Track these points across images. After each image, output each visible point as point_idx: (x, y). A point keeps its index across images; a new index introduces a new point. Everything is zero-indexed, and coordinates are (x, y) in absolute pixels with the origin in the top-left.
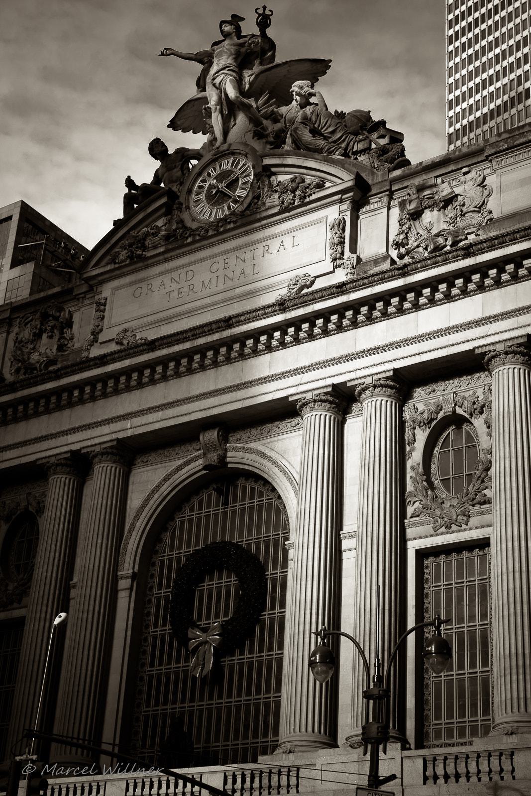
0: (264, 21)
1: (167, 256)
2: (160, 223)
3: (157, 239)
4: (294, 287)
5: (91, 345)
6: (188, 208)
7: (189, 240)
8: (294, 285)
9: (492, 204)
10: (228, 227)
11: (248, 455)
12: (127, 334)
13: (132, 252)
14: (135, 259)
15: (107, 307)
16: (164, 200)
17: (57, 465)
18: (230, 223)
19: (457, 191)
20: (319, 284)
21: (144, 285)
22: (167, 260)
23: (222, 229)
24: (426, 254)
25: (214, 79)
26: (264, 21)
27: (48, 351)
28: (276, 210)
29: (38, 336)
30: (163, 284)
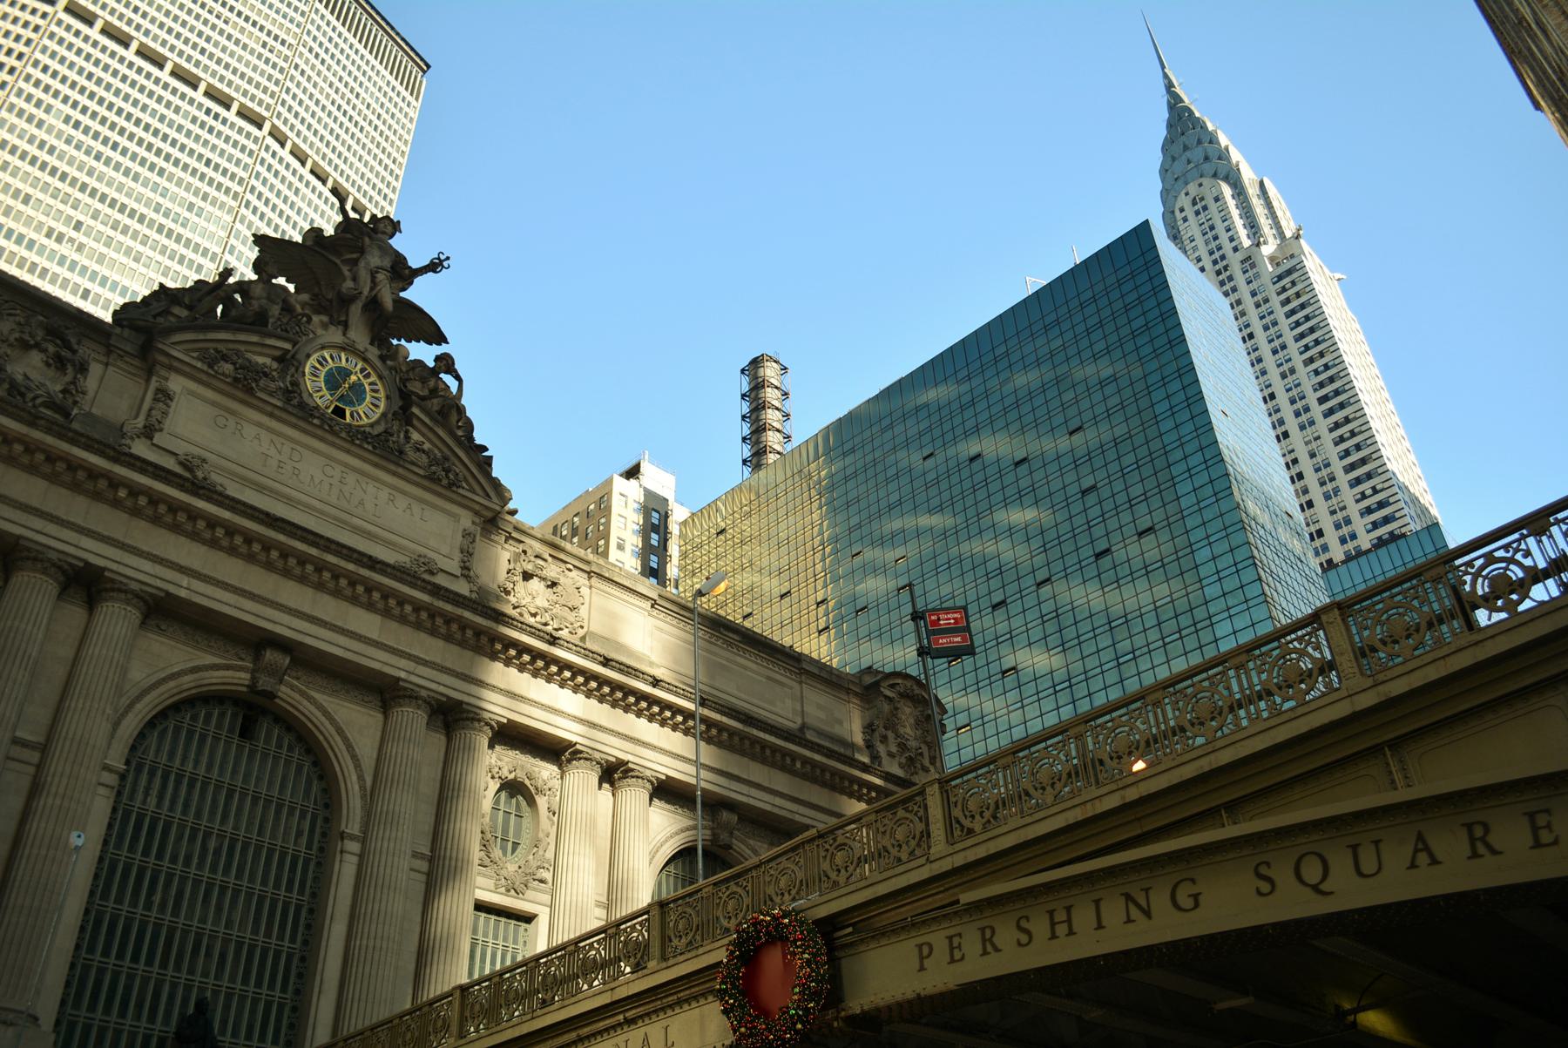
0: (435, 266)
1: (277, 412)
2: (268, 361)
3: (273, 385)
7: (316, 421)
9: (583, 611)
11: (305, 702)
15: (173, 405)
16: (287, 346)
17: (54, 565)
19: (562, 580)
20: (440, 580)
21: (232, 422)
22: (271, 415)
24: (532, 620)
26: (435, 266)
28: (421, 472)
29: (25, 346)
30: (257, 437)
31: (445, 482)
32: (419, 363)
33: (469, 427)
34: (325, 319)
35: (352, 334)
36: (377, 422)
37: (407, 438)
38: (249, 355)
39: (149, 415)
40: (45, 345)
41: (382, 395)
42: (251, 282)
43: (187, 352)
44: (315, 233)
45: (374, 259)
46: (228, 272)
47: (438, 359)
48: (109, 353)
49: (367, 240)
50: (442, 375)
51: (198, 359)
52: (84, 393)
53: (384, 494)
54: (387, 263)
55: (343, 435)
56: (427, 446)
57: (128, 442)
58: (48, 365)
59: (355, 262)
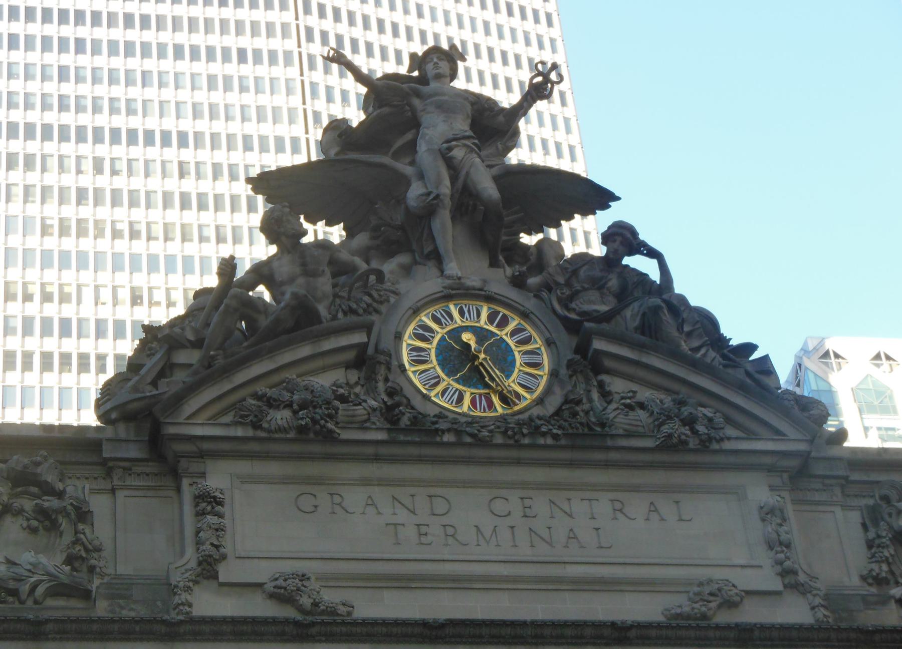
1: (383, 450)
2: (338, 375)
3: (360, 411)
4: (711, 598)
5: (196, 582)
6: (403, 370)
7: (448, 438)
8: (711, 594)
10: (541, 441)
12: (305, 583)
13: (315, 422)
14: (312, 435)
18: (544, 434)
22: (377, 458)
23: (526, 441)
25: (450, 149)
27: (43, 559)
28: (648, 443)
30: (371, 503)
31: (693, 443)
32: (583, 259)
33: (706, 323)
34: (403, 259)
35: (452, 268)
36: (548, 391)
37: (606, 395)
38: (303, 382)
39: (199, 543)
40: (17, 503)
41: (538, 343)
42: (271, 260)
43: (213, 420)
44: (337, 130)
45: (436, 129)
46: (228, 267)
47: (606, 238)
48: (109, 473)
49: (416, 102)
50: (627, 261)
51: (235, 424)
52: (98, 550)
53: (603, 506)
54: (462, 125)
55: (499, 439)
56: (645, 394)
57: (184, 596)
58: (34, 531)
59: (411, 147)
